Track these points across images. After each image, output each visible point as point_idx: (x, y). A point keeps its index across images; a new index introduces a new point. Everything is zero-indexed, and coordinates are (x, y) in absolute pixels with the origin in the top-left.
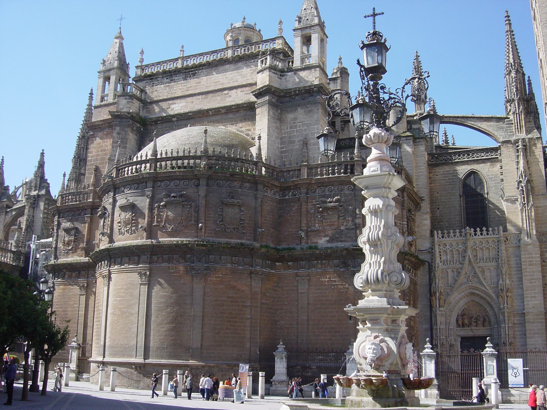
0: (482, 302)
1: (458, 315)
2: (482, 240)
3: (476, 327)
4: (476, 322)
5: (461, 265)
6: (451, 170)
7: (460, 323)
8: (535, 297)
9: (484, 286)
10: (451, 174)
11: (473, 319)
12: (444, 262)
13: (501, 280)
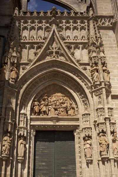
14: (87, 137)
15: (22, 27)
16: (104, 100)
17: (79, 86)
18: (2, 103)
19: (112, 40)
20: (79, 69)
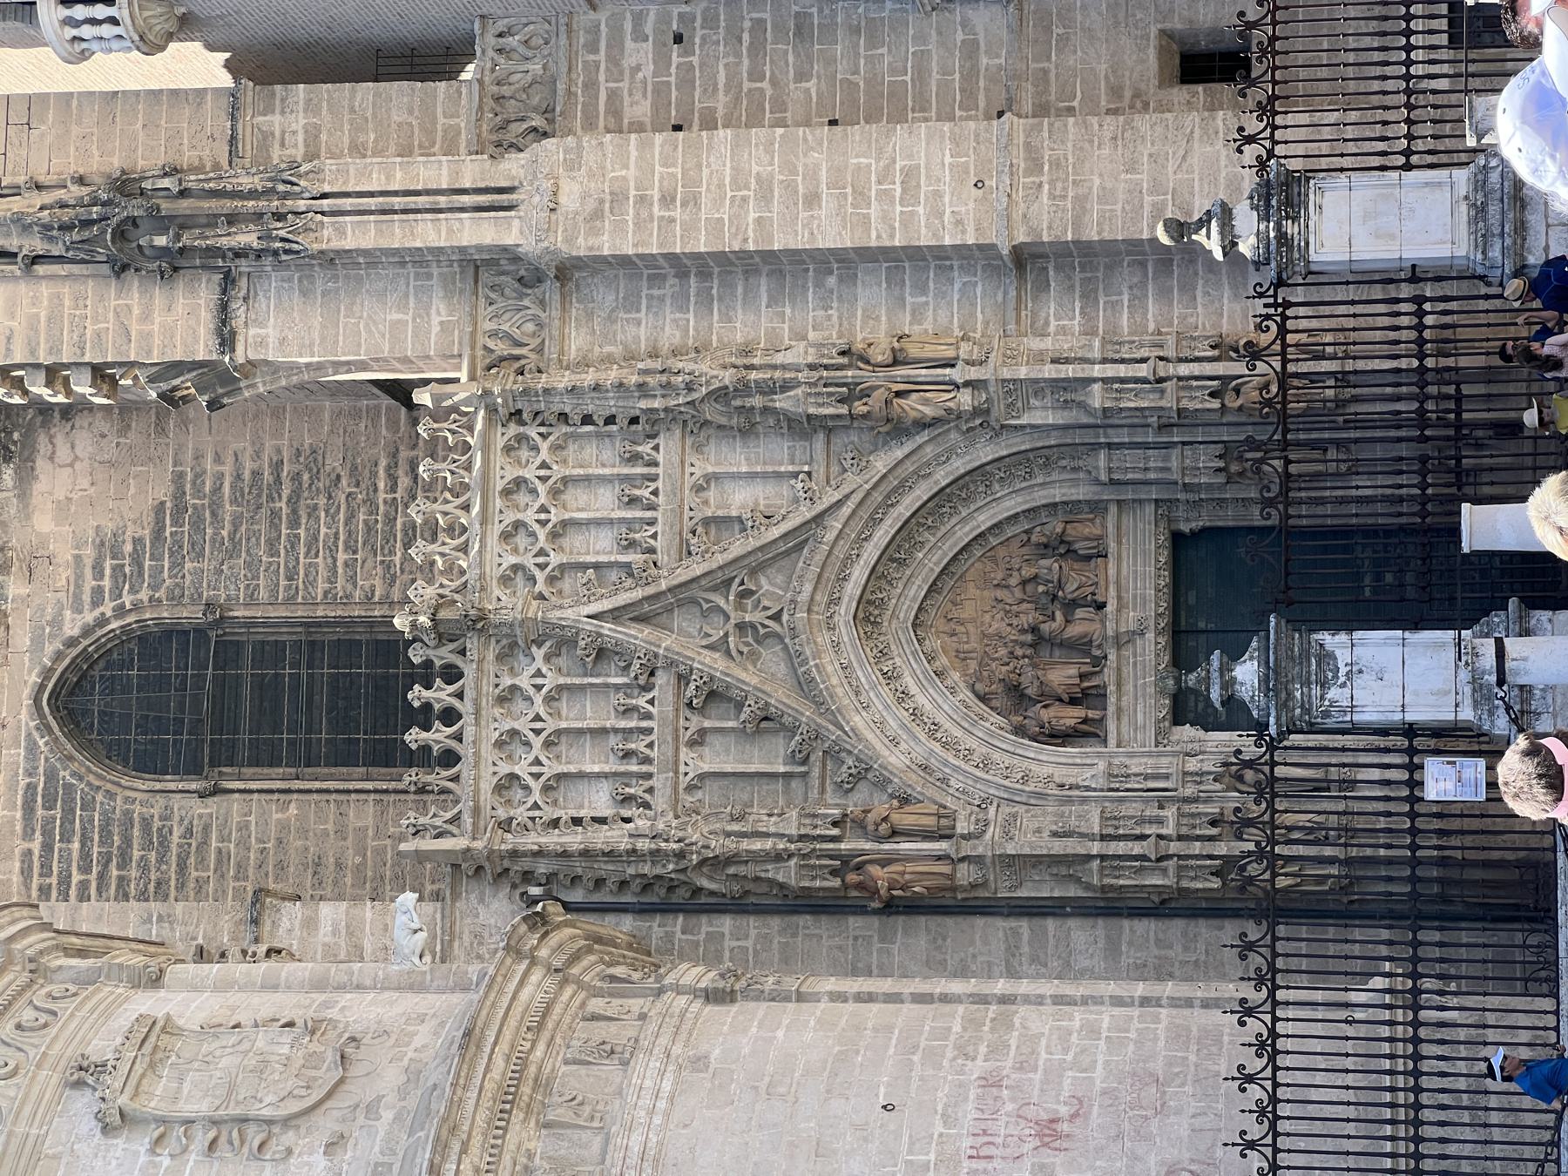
0: (929, 561)
1: (1019, 731)
2: (497, 529)
3: (1101, 606)
4: (1071, 605)
5: (661, 679)
6: (20, 846)
7: (1070, 716)
8: (909, 175)
9: (818, 519)
10: (47, 847)
11: (1046, 628)
12: (627, 800)
13: (781, 402)
19: (656, 292)
20: (867, 487)
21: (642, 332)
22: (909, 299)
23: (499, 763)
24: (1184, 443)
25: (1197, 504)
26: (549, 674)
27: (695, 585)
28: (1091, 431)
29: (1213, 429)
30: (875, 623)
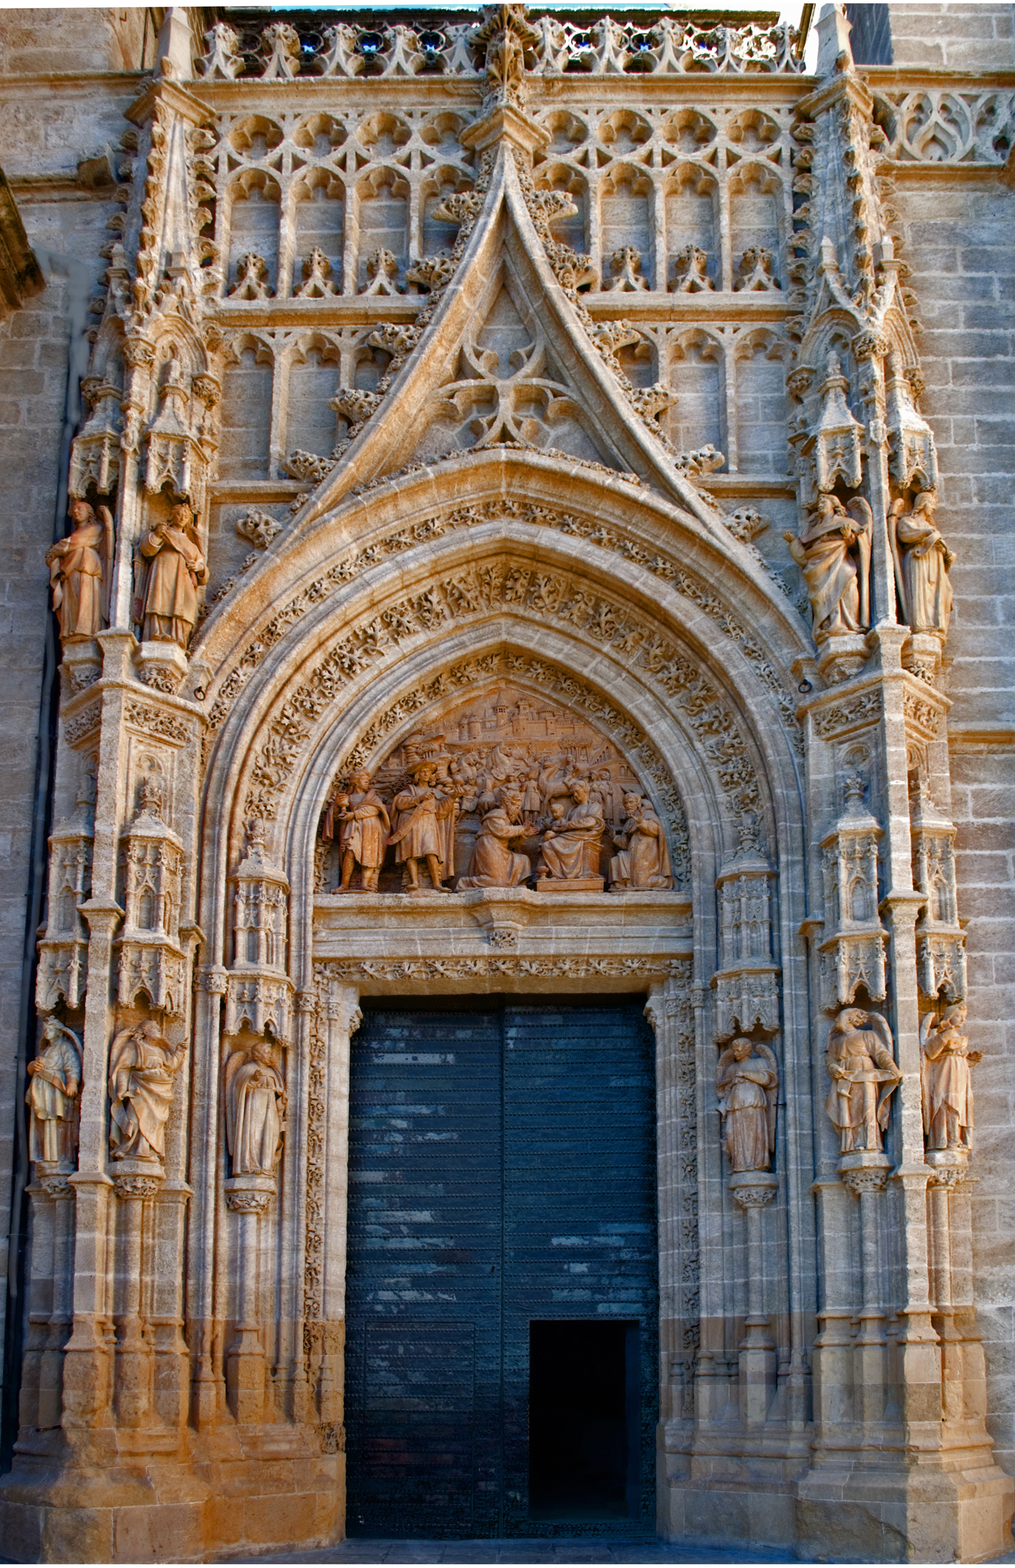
3: (531, 884)
14: (747, 1035)
15: (225, 177)
16: (891, 772)
17: (703, 667)
18: (93, 804)
19: (996, 288)
21: (934, 274)
22: (999, 599)
23: (298, 123)
24: (779, 975)
25: (687, 1011)
26: (425, 172)
27: (552, 332)
28: (798, 843)
29: (803, 1009)
30: (503, 589)
